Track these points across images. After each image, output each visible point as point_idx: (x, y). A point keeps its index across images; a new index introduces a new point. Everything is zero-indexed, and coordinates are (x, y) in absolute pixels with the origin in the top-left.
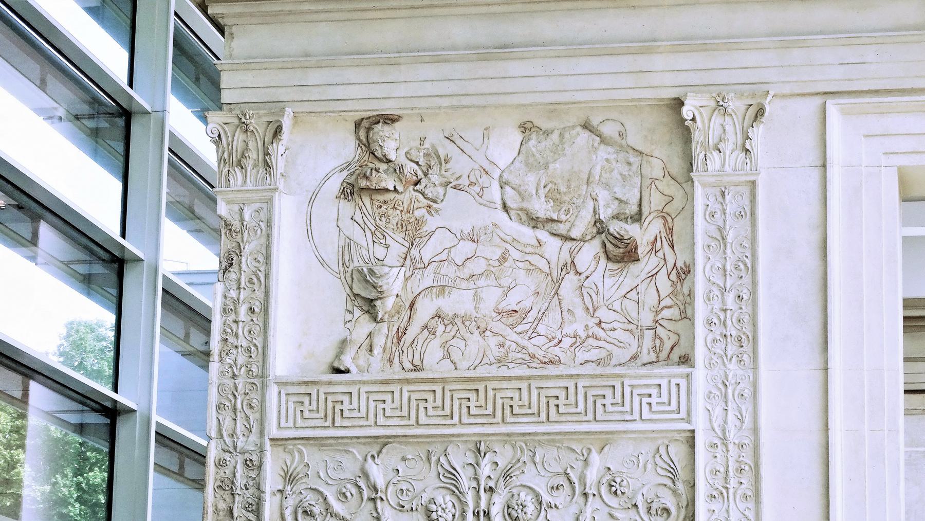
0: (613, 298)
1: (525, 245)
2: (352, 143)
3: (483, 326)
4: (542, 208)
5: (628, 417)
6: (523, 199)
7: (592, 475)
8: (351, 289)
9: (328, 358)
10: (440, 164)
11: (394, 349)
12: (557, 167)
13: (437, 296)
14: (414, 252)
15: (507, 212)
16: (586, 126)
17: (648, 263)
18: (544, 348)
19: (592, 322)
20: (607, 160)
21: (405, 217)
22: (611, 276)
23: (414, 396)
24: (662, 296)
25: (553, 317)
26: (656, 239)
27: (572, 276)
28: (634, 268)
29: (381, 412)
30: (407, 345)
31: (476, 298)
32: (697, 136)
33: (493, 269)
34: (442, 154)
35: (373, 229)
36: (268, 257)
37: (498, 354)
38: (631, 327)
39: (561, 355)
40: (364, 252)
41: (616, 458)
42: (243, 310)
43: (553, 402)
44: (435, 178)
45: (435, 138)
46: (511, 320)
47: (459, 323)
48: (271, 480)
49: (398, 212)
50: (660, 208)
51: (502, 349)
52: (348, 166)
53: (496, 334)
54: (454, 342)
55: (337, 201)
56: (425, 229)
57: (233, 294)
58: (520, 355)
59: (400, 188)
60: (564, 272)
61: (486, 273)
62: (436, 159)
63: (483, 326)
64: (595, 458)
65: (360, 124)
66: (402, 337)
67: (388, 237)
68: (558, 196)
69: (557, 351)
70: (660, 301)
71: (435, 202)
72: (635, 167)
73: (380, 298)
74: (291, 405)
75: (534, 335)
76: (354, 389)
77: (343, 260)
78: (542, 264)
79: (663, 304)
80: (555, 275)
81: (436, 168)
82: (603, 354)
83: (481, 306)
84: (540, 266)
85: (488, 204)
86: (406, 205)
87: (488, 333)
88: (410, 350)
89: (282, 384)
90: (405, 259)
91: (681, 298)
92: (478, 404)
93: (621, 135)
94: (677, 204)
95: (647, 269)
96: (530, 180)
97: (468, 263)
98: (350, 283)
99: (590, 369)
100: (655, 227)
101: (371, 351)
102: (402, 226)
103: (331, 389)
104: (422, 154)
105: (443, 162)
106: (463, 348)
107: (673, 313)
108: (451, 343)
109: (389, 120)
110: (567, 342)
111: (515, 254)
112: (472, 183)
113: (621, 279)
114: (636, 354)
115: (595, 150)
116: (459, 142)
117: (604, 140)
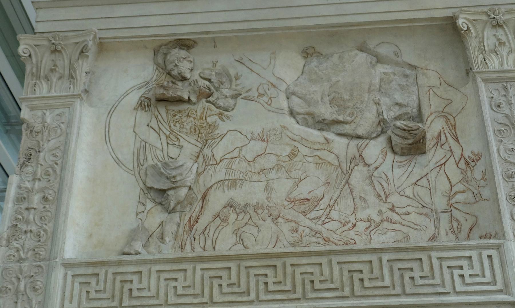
0: (404, 186)
1: (314, 143)
3: (275, 213)
4: (326, 112)
5: (441, 290)
6: (309, 105)
8: (144, 184)
10: (231, 81)
11: (186, 236)
13: (229, 188)
15: (294, 117)
16: (362, 49)
17: (434, 156)
18: (338, 232)
19: (385, 208)
20: (385, 73)
21: (198, 123)
22: (399, 167)
23: (208, 274)
24: (454, 182)
25: (346, 203)
26: (440, 134)
27: (361, 167)
28: (421, 159)
29: (173, 290)
30: (199, 232)
31: (268, 189)
33: (283, 164)
34: (232, 72)
35: (168, 133)
37: (291, 239)
38: (425, 211)
39: (356, 237)
40: (159, 153)
42: (36, 200)
43: (356, 276)
44: (226, 91)
47: (251, 212)
49: (192, 119)
50: (441, 109)
51: (295, 235)
52: (146, 85)
53: (288, 221)
54: (246, 229)
55: (135, 112)
56: (217, 132)
58: (314, 239)
59: (193, 99)
60: (353, 165)
61: (278, 167)
63: (275, 213)
65: (158, 51)
66: (194, 225)
67: (181, 140)
68: (342, 103)
69: (352, 233)
70: (451, 187)
71: (227, 110)
72: (411, 80)
73: (173, 188)
74: (77, 285)
75: (327, 220)
76: (143, 269)
77: (138, 160)
78: (331, 158)
79: (455, 189)
80: (344, 166)
81: (227, 85)
82: (400, 236)
83: (273, 195)
84: (329, 159)
85: (276, 110)
86: (199, 114)
87: (280, 220)
88: (202, 238)
89: (68, 265)
90: (198, 157)
91: (473, 183)
92: (276, 280)
93: (396, 54)
95: (434, 160)
96: (316, 91)
97: (259, 159)
98: (144, 178)
101: (162, 238)
102: (195, 131)
103: (120, 270)
104: (214, 73)
105: (234, 80)
106: (256, 234)
107: (468, 196)
108: (243, 229)
110: (361, 226)
111: (304, 150)
112: (260, 95)
113: (410, 169)
114: (434, 235)
115: (373, 66)
116: (248, 63)
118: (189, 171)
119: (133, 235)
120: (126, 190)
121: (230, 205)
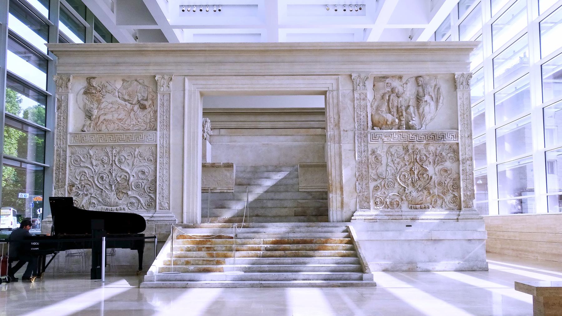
2: (86, 82)
4: (126, 97)
7: (136, 153)
9: (81, 128)
12: (130, 89)
16: (136, 80)
28: (146, 110)
32: (158, 84)
36: (67, 107)
41: (141, 150)
42: (62, 118)
45: (103, 82)
48: (68, 154)
62: (104, 87)
64: (137, 150)
78: (127, 109)
89: (70, 134)
94: (155, 97)
96: (124, 92)
99: (136, 131)
100: (150, 102)
102: (97, 101)
109: (94, 78)
110: (132, 125)
115: (138, 85)
117: (140, 83)
118: (95, 112)
119: (84, 126)
120: (82, 115)
121: (104, 120)
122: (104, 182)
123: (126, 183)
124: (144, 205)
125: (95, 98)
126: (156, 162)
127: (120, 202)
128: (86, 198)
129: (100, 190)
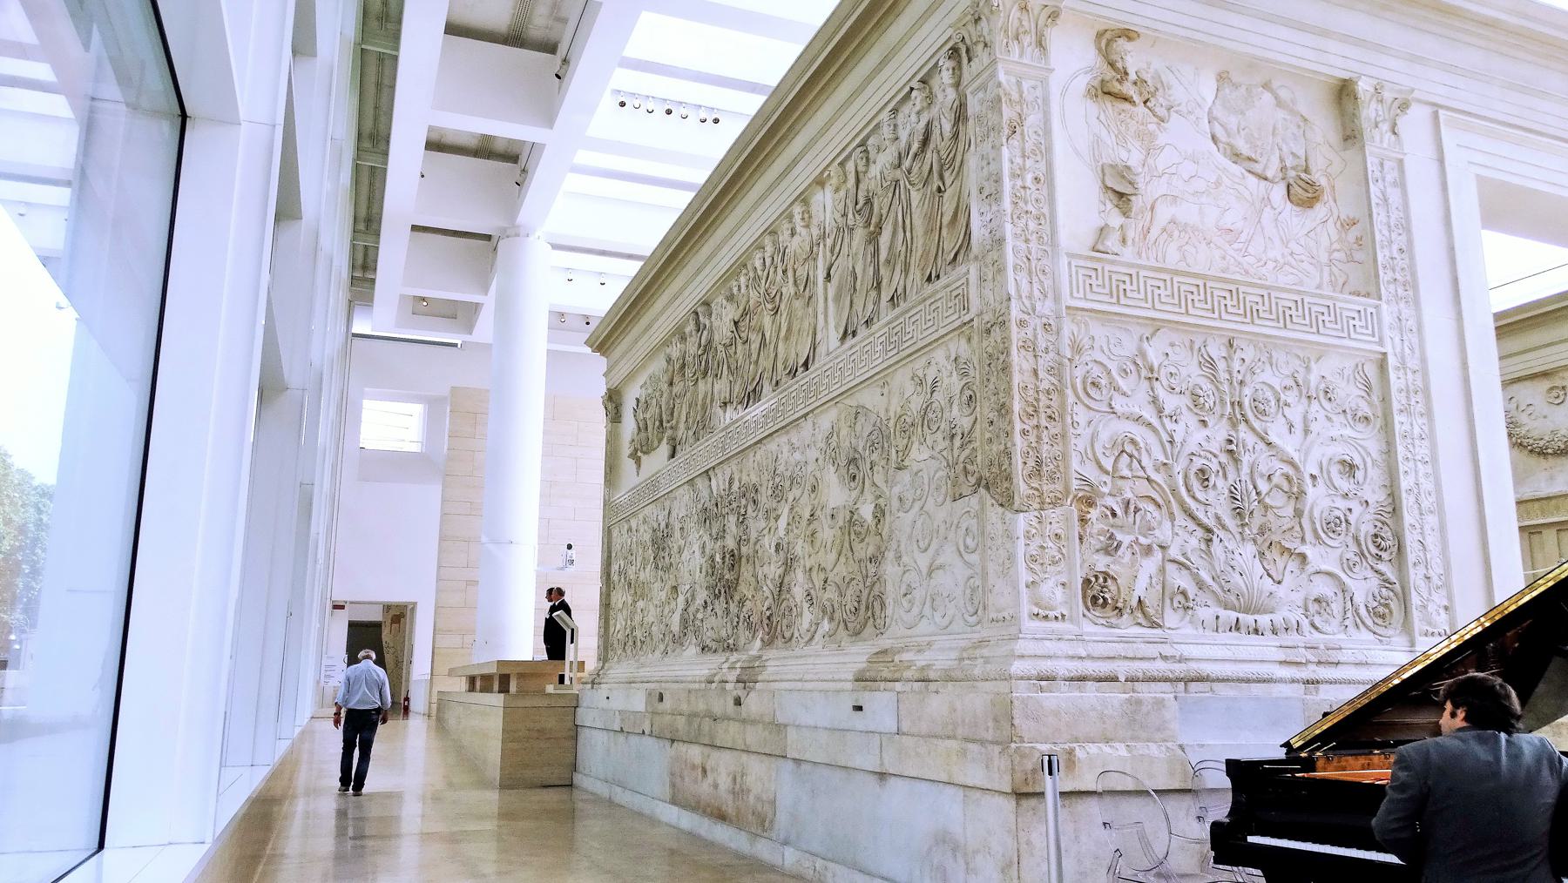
14: (1150, 161)
17: (1320, 210)
27: (1268, 209)
28: (1310, 212)
46: (1228, 238)
57: (1019, 160)
69: (1264, 270)
78: (1247, 194)
89: (1071, 255)
102: (1140, 136)
110: (1271, 265)
121: (1173, 221)
122: (1211, 495)
123: (1289, 511)
124: (1363, 611)
125: (1133, 126)
126: (1387, 427)
127: (1281, 591)
128: (1150, 565)
129: (1200, 533)
